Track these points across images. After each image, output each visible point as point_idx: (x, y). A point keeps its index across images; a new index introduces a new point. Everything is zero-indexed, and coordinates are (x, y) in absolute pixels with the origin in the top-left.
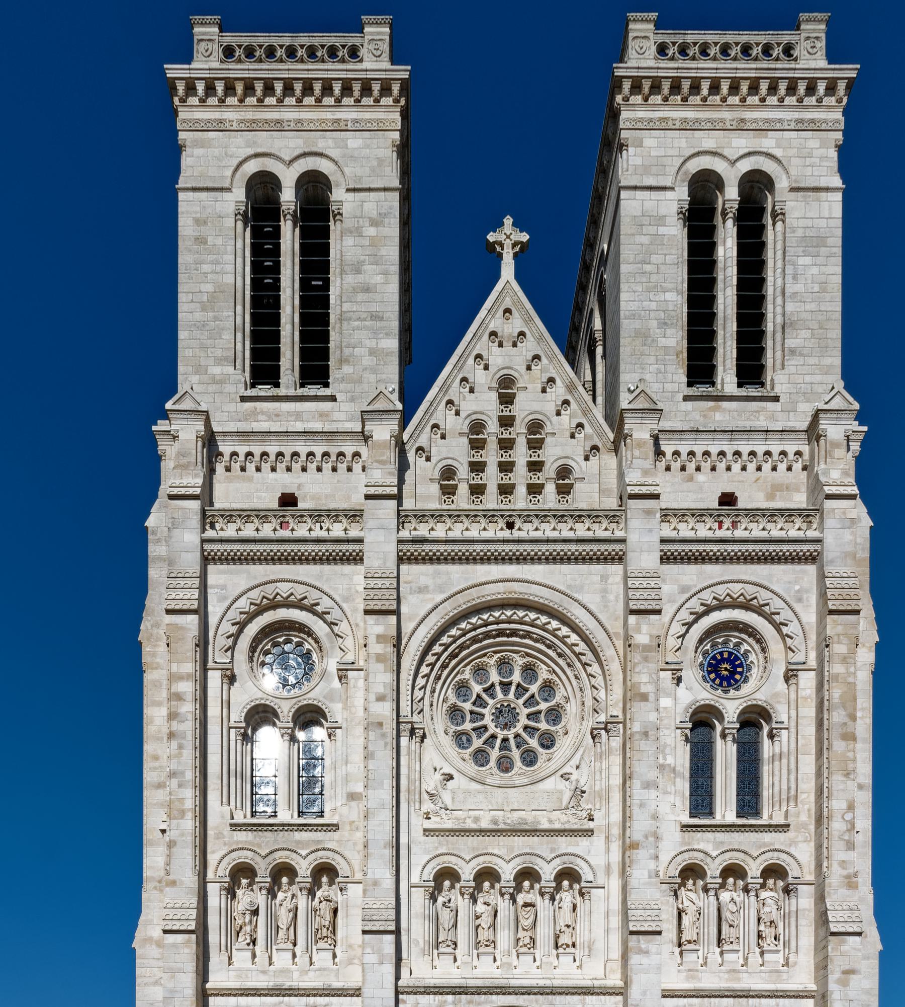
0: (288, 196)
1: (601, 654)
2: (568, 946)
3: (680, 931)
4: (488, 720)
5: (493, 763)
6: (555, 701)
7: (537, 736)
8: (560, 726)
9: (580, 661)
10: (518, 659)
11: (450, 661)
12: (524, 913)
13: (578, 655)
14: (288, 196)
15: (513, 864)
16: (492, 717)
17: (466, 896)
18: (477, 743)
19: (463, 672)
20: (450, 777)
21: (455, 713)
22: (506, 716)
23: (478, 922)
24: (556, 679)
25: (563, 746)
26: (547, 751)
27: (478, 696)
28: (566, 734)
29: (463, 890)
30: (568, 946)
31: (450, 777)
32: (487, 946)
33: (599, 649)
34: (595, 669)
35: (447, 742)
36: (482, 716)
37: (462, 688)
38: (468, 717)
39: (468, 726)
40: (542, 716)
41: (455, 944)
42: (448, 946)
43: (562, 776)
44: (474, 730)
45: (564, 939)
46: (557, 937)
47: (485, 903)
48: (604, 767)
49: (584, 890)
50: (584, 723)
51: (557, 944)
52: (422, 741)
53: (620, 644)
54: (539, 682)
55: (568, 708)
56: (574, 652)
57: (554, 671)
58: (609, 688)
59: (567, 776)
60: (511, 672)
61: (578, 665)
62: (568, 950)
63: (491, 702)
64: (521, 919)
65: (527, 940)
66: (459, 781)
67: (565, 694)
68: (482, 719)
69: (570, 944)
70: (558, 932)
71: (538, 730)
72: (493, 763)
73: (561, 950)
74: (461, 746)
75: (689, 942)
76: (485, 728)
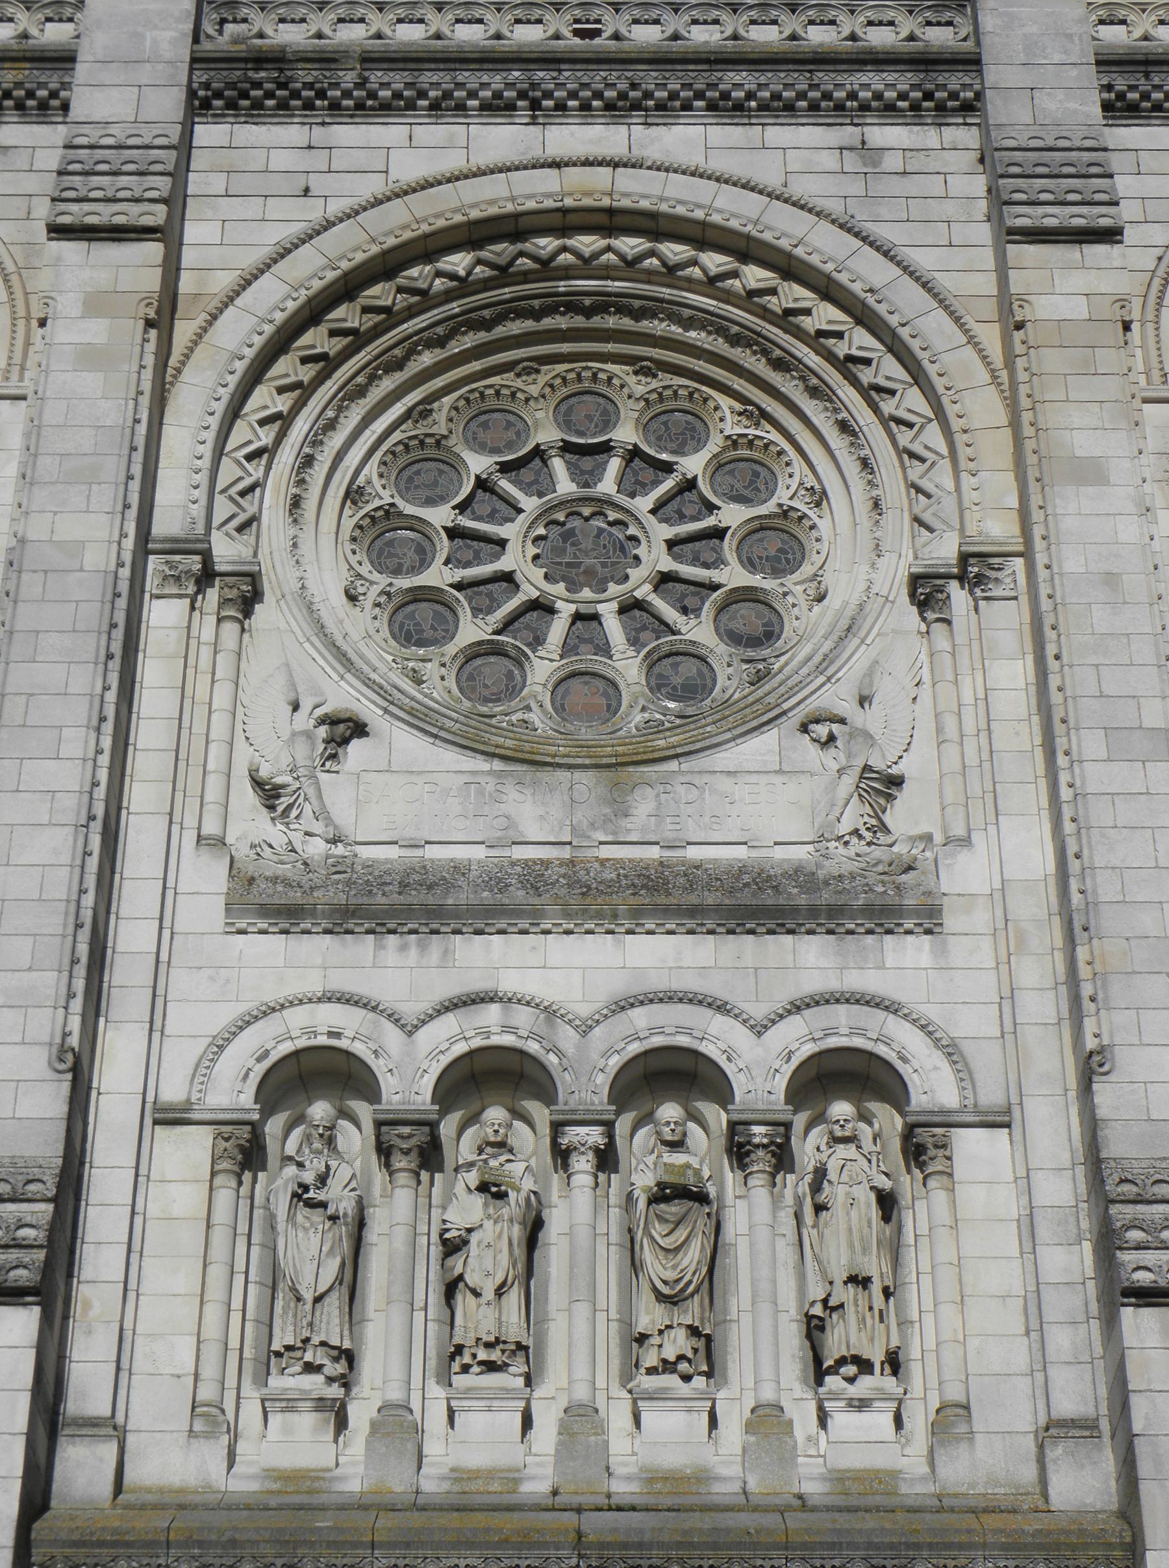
1: (932, 370)
2: (865, 1366)
6: (774, 501)
7: (708, 609)
8: (796, 576)
9: (855, 382)
10: (632, 380)
11: (373, 378)
12: (658, 1229)
13: (848, 365)
16: (532, 550)
17: (400, 1162)
19: (426, 414)
20: (359, 729)
23: (457, 1264)
24: (774, 436)
28: (820, 598)
29: (391, 1134)
30: (865, 1366)
31: (359, 729)
32: (490, 1367)
33: (923, 356)
34: (913, 401)
40: (728, 546)
41: (349, 1357)
42: (311, 1368)
43: (804, 728)
44: (459, 586)
46: (814, 1328)
47: (483, 1188)
48: (968, 697)
49: (922, 1135)
50: (881, 563)
51: (818, 1360)
52: (248, 613)
53: (991, 336)
54: (714, 444)
55: (824, 525)
56: (830, 357)
57: (764, 415)
58: (963, 452)
59: (822, 730)
60: (609, 421)
61: (848, 394)
62: (866, 1385)
64: (648, 1255)
65: (677, 1344)
67: (810, 481)
68: (496, 557)
69: (877, 1357)
70: (818, 1310)
71: (715, 587)
73: (833, 1382)
74: (408, 636)
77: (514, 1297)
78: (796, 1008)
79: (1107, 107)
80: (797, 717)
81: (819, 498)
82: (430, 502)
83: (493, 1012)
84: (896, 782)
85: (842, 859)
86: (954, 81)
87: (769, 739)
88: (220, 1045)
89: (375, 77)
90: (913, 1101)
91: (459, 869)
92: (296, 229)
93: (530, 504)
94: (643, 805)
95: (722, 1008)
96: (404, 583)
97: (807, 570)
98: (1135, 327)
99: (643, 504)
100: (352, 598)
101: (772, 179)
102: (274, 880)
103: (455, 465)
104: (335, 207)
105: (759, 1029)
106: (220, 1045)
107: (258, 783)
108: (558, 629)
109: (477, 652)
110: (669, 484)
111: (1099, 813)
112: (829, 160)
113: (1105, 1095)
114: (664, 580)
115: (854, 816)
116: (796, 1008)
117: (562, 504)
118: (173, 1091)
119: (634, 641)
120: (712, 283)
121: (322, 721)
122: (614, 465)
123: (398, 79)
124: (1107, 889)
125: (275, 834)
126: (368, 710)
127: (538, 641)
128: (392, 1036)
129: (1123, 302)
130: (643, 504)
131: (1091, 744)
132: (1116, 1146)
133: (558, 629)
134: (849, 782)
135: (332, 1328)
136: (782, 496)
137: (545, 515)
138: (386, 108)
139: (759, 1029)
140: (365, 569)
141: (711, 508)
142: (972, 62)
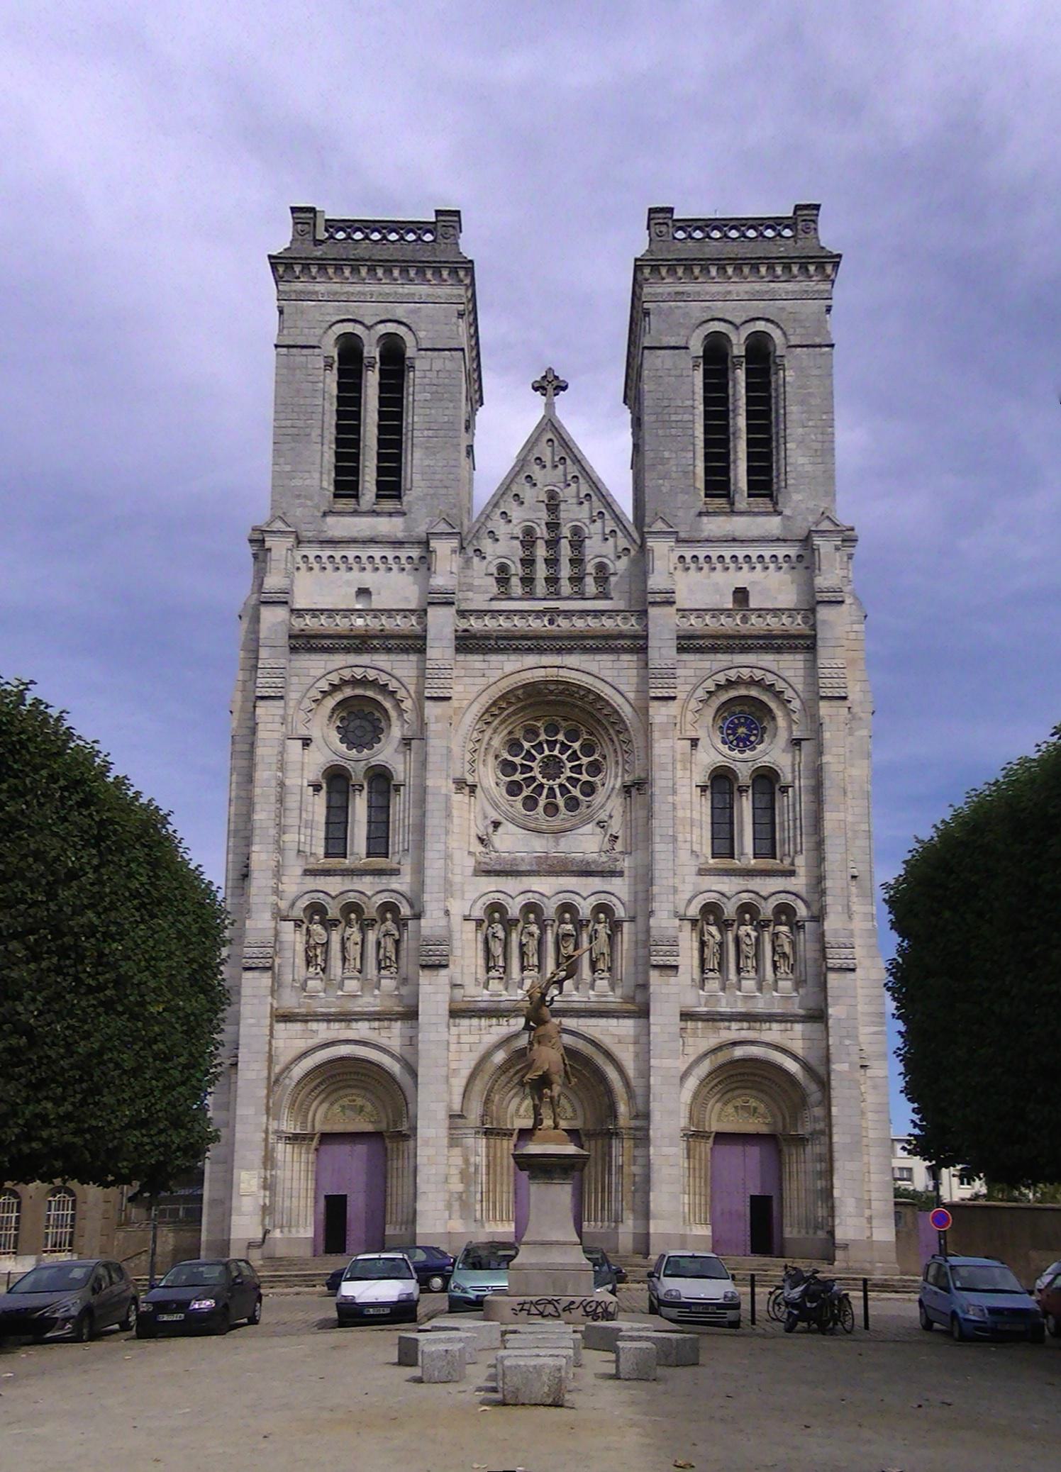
0: (372, 351)
2: (603, 971)
3: (703, 961)
4: (536, 772)
5: (540, 809)
14: (372, 351)
15: (554, 899)
18: (526, 792)
21: (508, 767)
22: (551, 768)
25: (598, 798)
26: (587, 799)
27: (528, 752)
30: (603, 971)
35: (500, 793)
36: (531, 769)
37: (514, 746)
38: (519, 768)
39: (518, 777)
45: (601, 965)
63: (539, 757)
66: (507, 827)
72: (540, 809)
75: (711, 970)
76: (534, 779)
77: (536, 956)
78: (593, 894)
79: (678, 649)
80: (597, 820)
81: (604, 757)
82: (516, 756)
83: (530, 895)
84: (617, 837)
85: (604, 859)
86: (641, 642)
87: (590, 826)
88: (475, 902)
89: (500, 642)
90: (617, 915)
91: (523, 860)
92: (483, 687)
93: (539, 757)
94: (563, 841)
95: (578, 894)
96: (508, 779)
97: (600, 776)
98: (678, 725)
99: (564, 757)
100: (497, 784)
101: (595, 672)
102: (485, 863)
103: (521, 747)
104: (492, 680)
105: (585, 899)
106: (475, 902)
107: (479, 838)
108: (545, 792)
109: (527, 797)
110: (570, 752)
111: (657, 856)
112: (609, 664)
113: (652, 922)
114: (569, 779)
115: (607, 846)
116: (593, 894)
117: (546, 757)
118: (467, 913)
119: (562, 795)
120: (581, 698)
121: (493, 822)
122: (558, 746)
123: (505, 642)
124: (657, 874)
125: (484, 849)
126: (500, 819)
127: (540, 795)
128: (510, 900)
129: (675, 717)
130: (564, 757)
131: (657, 839)
132: (654, 932)
133: (545, 792)
134: (606, 839)
135: (501, 963)
136: (596, 756)
137: (542, 761)
138: (502, 649)
139: (585, 899)
140: (500, 775)
141: (579, 759)
142: (646, 638)
